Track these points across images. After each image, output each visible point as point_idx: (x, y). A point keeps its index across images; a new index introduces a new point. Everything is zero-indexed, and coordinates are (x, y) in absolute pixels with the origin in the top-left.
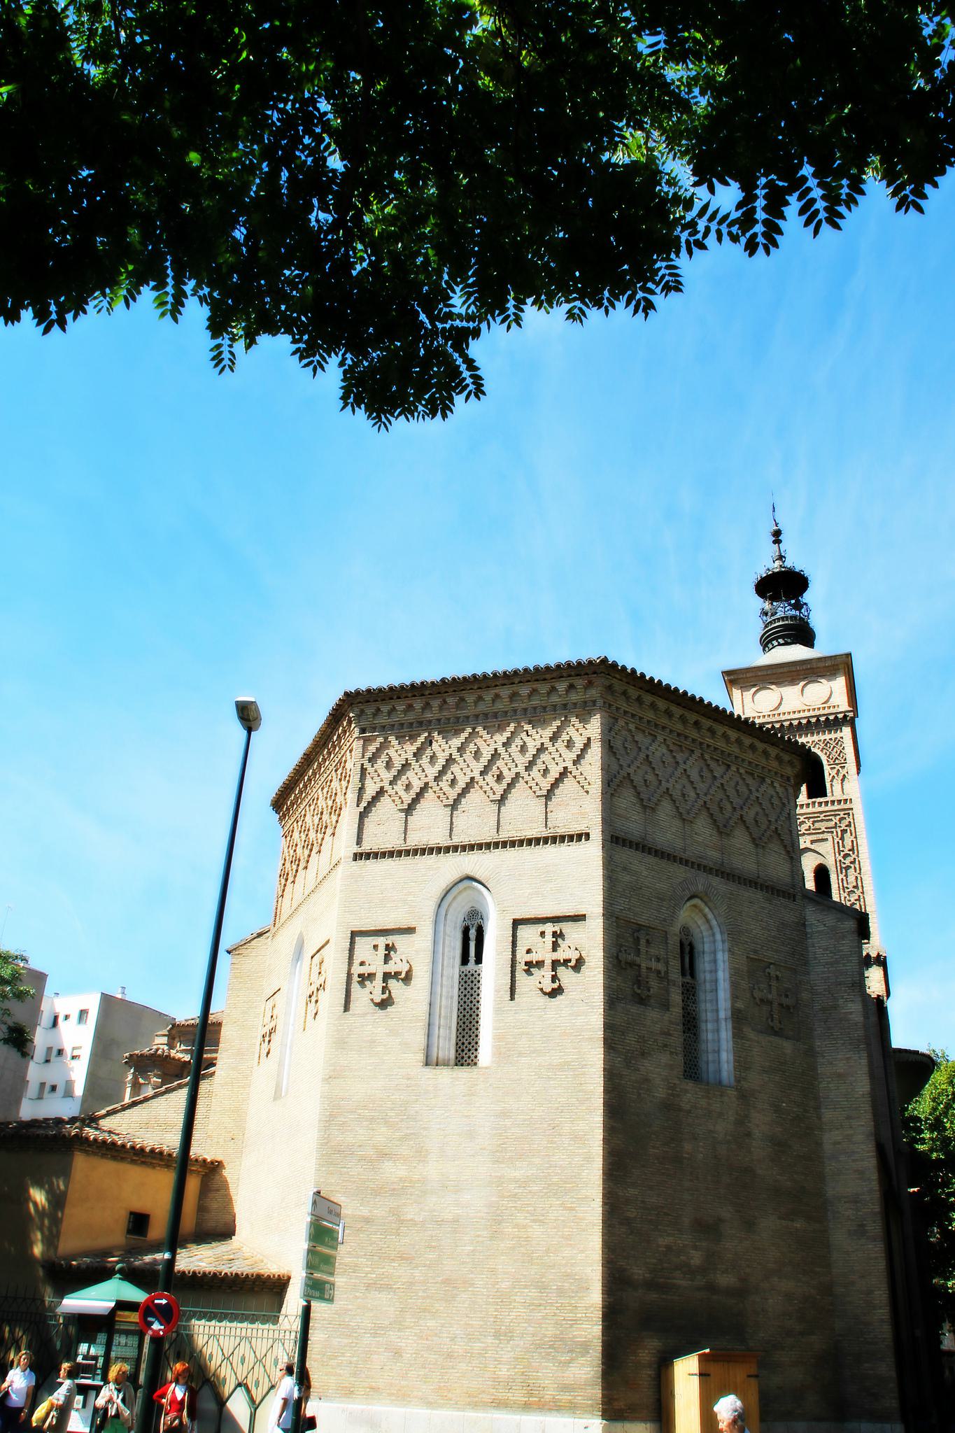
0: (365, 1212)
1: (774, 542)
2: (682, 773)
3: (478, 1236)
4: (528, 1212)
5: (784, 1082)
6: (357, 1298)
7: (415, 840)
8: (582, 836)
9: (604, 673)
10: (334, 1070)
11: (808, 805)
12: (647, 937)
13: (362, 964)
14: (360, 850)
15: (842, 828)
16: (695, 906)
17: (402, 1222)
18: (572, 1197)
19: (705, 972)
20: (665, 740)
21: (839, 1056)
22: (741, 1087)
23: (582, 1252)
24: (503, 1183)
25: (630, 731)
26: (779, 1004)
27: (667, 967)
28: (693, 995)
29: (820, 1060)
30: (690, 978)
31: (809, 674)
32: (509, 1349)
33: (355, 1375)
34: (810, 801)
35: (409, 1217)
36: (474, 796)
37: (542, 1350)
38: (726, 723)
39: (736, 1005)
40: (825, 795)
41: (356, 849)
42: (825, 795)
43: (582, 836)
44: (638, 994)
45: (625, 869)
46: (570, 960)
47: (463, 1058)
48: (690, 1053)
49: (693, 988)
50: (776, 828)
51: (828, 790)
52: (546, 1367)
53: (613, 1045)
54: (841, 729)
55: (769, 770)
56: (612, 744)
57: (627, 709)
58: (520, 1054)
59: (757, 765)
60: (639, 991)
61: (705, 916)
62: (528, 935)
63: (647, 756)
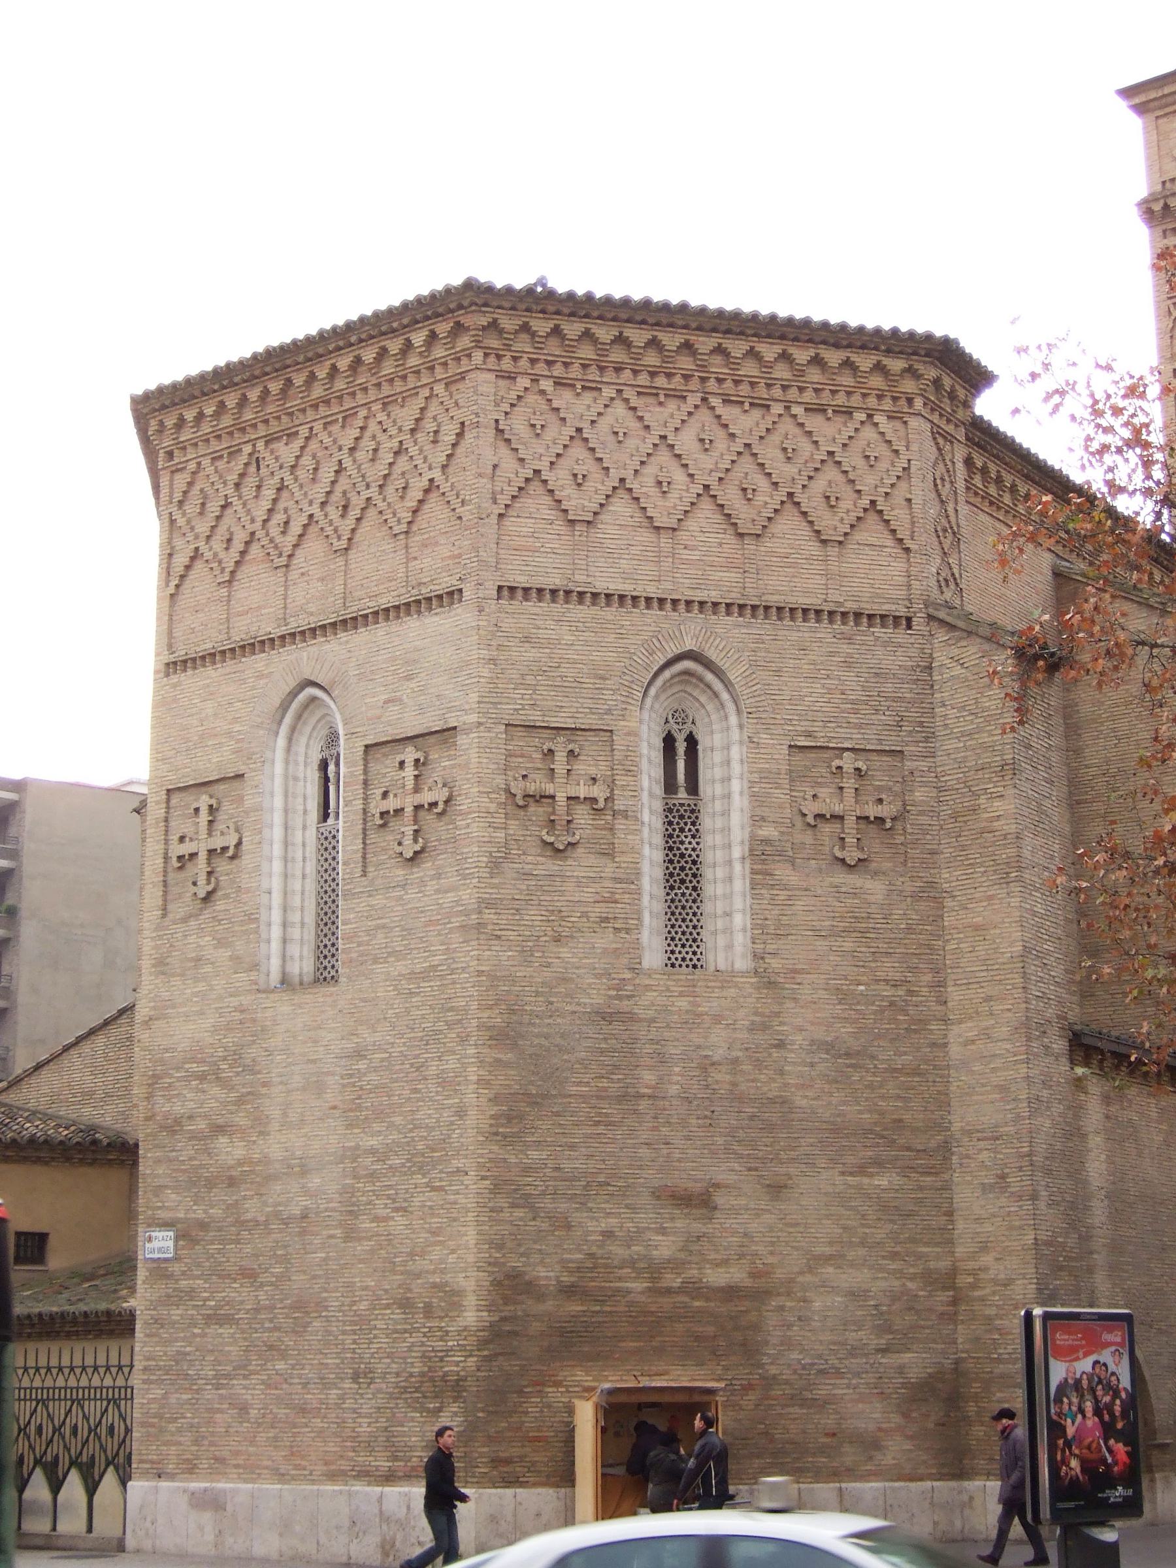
0: (200, 1215)
2: (655, 445)
3: (332, 1237)
4: (389, 1197)
5: (863, 949)
6: (195, 1336)
7: (242, 630)
8: (453, 595)
9: (476, 304)
10: (154, 1008)
12: (570, 747)
13: (182, 839)
14: (172, 658)
16: (686, 672)
17: (241, 1223)
18: (441, 1172)
19: (714, 781)
20: (619, 391)
21: (977, 895)
22: (765, 969)
23: (453, 1252)
24: (359, 1156)
25: (542, 392)
26: (858, 818)
27: (612, 790)
28: (693, 824)
29: (949, 903)
30: (685, 795)
32: (370, 1396)
33: (196, 1442)
35: (249, 1216)
36: (314, 547)
37: (408, 1396)
38: (749, 332)
39: (761, 832)
41: (168, 658)
43: (453, 595)
44: (552, 844)
45: (527, 639)
46: (435, 804)
47: (325, 968)
48: (684, 920)
49: (693, 811)
50: (873, 502)
52: (413, 1419)
53: (499, 933)
56: (501, 427)
57: (535, 356)
58: (375, 961)
60: (551, 839)
61: (709, 686)
62: (385, 768)
63: (579, 430)
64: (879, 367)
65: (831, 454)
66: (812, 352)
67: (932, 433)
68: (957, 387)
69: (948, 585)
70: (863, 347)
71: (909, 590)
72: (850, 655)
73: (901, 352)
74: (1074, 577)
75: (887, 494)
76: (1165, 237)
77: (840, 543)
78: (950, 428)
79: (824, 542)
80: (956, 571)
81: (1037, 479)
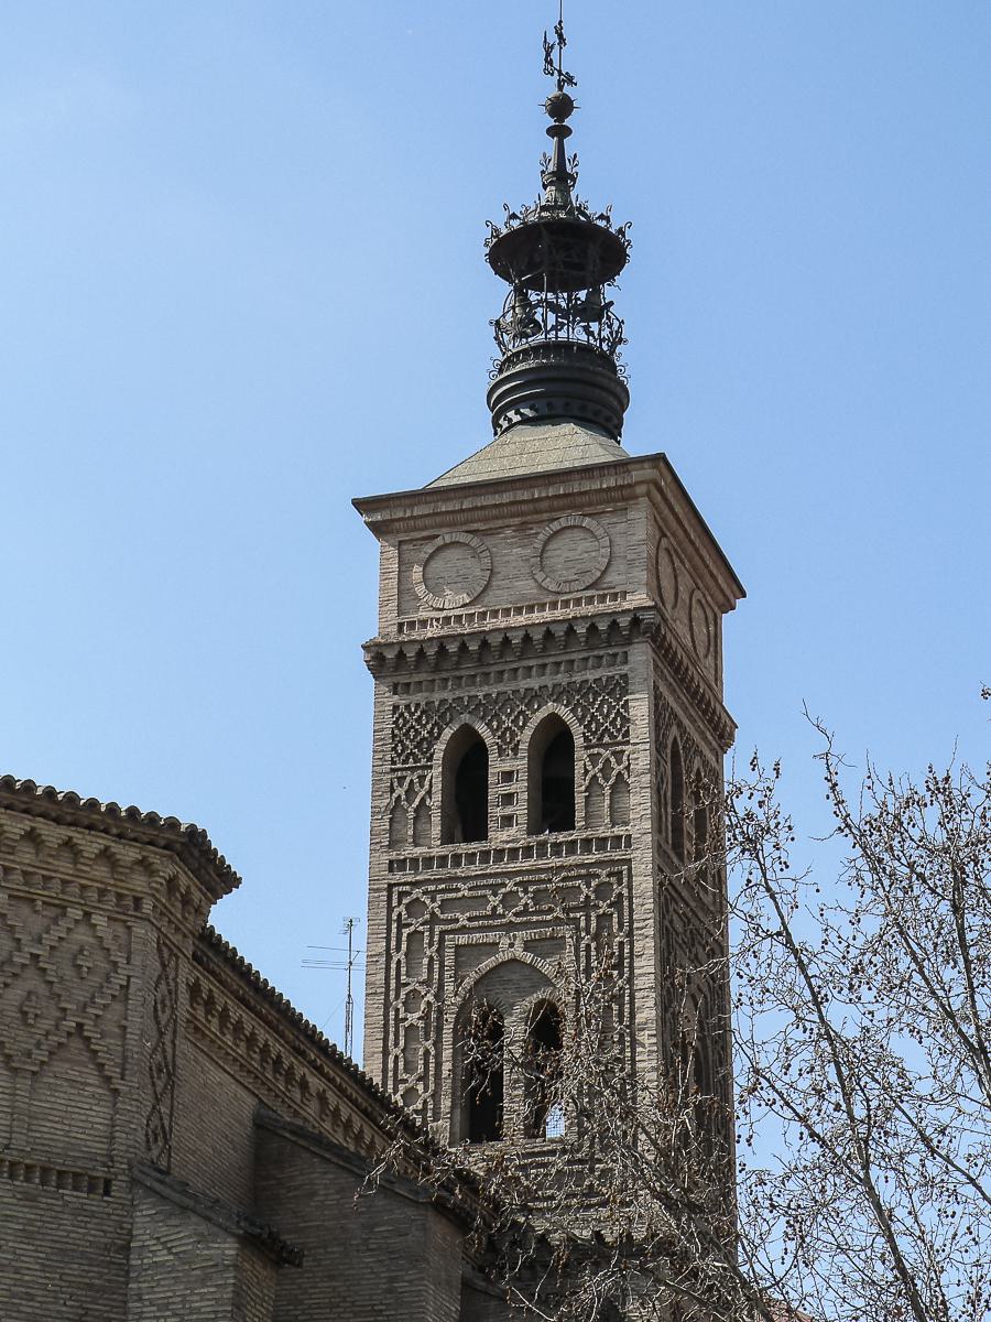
1: (551, 132)
11: (528, 851)
15: (601, 911)
31: (562, 509)
34: (533, 840)
40: (568, 824)
42: (568, 824)
50: (80, 1026)
51: (579, 814)
54: (626, 652)
55: (83, 887)
59: (46, 879)
64: (106, 855)
65: (35, 957)
66: (27, 825)
67: (158, 943)
68: (193, 889)
69: (156, 1140)
70: (90, 827)
71: (111, 1144)
72: (30, 1222)
73: (135, 840)
74: (281, 1132)
75: (97, 1016)
76: (395, 693)
77: (34, 1073)
78: (177, 939)
79: (15, 1071)
80: (166, 1123)
81: (252, 1002)
